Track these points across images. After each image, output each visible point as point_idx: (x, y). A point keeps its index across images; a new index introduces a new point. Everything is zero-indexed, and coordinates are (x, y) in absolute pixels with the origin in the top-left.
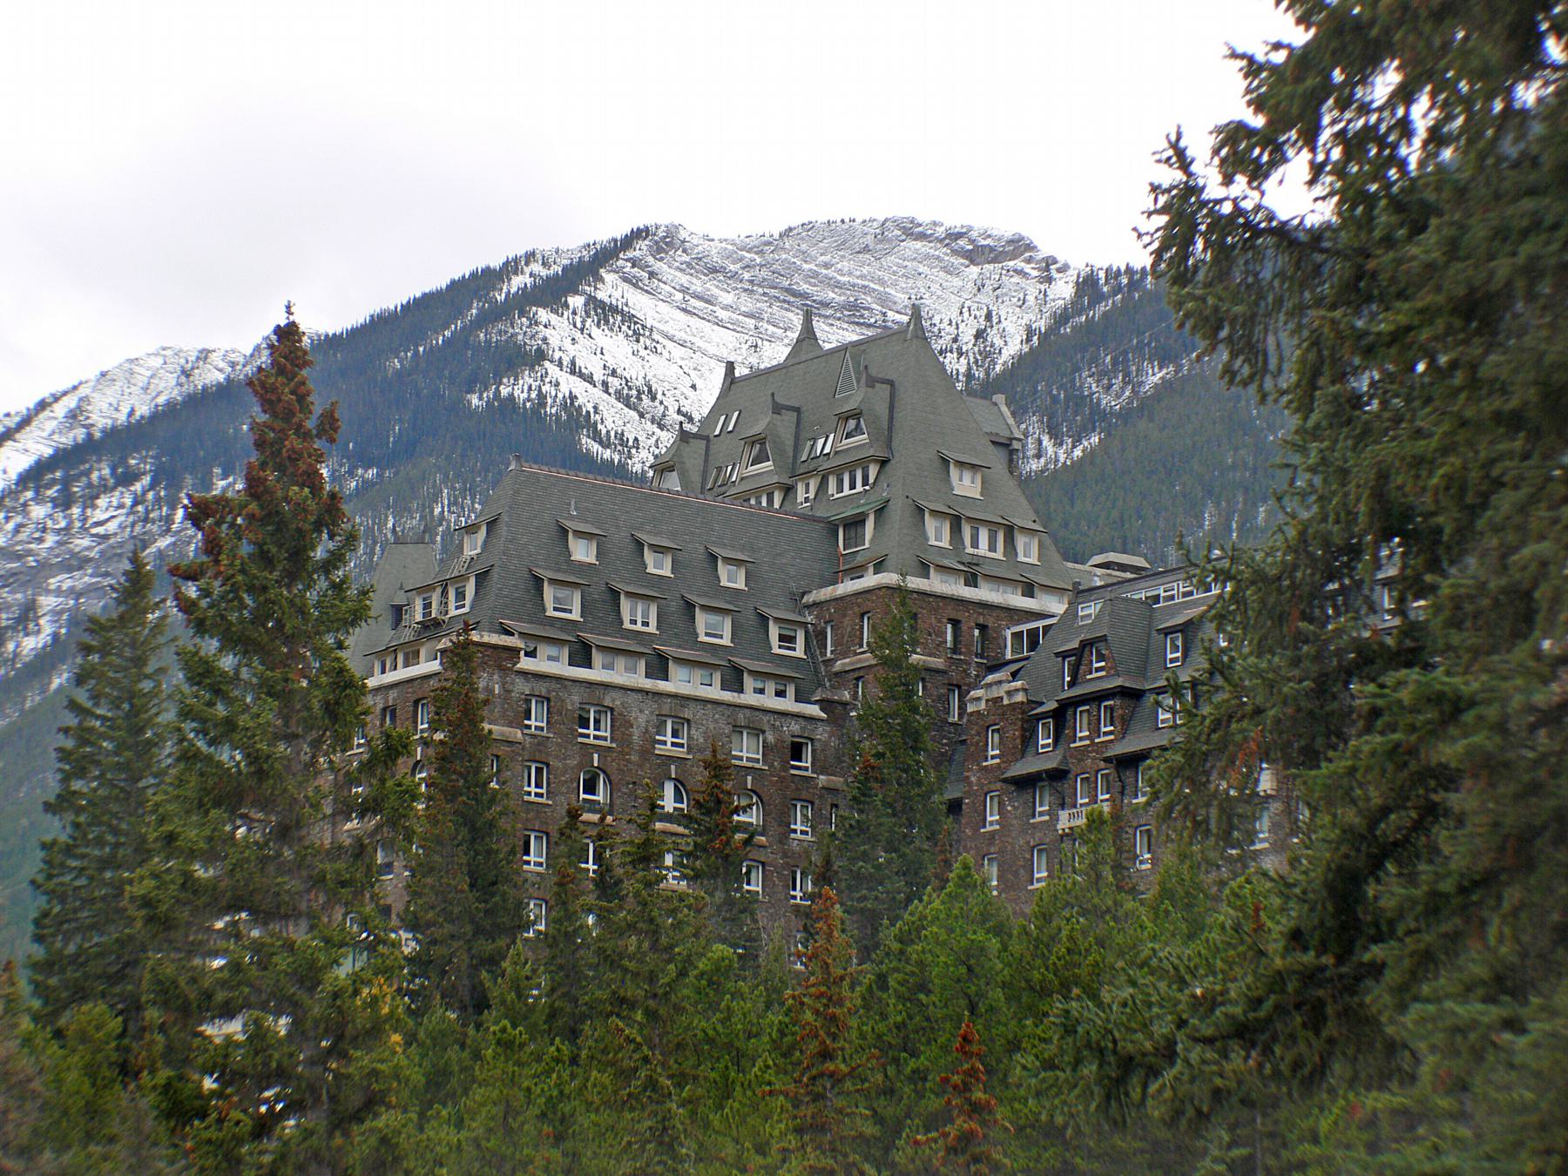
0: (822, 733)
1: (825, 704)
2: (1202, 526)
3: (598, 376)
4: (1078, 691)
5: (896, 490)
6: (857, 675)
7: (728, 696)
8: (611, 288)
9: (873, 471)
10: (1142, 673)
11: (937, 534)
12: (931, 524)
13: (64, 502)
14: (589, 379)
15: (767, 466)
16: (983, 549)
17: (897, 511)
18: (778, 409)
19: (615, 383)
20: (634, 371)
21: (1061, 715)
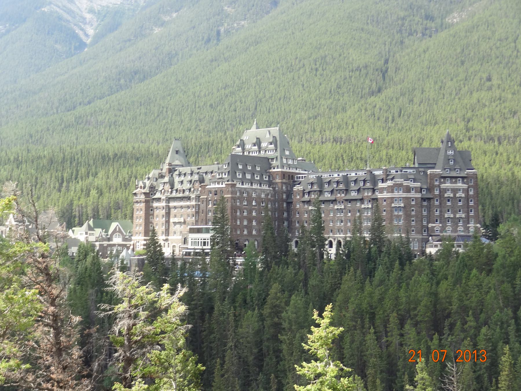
1: (272, 188)
4: (312, 190)
11: (285, 161)
14: (59, 7)
18: (257, 138)
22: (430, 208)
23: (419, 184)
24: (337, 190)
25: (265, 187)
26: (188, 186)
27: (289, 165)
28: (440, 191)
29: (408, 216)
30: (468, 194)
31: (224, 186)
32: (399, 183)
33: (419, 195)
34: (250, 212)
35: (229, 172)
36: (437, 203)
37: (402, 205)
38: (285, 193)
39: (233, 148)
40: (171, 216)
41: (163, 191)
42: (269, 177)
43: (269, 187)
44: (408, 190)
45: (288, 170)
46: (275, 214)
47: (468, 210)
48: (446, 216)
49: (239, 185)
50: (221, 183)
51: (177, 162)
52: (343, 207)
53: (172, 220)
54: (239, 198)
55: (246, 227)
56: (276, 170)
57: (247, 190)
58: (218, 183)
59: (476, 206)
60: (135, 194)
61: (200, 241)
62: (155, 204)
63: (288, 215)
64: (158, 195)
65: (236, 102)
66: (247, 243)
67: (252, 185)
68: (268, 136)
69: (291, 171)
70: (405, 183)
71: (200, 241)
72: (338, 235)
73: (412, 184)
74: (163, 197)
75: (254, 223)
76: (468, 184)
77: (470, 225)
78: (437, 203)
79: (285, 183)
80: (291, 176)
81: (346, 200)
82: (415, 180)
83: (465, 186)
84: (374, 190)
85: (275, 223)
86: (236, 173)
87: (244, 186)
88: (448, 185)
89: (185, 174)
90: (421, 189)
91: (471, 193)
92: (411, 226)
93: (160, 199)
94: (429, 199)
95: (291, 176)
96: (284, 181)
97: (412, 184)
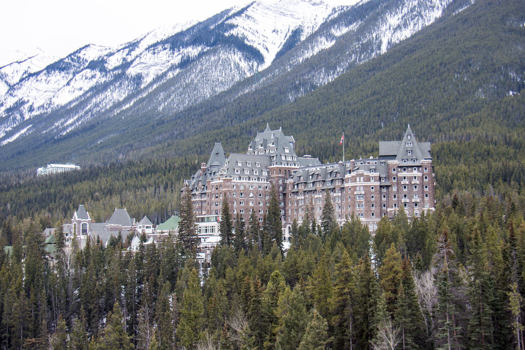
0: (269, 185)
1: (270, 181)
3: (248, 29)
6: (274, 178)
7: (258, 182)
8: (249, 12)
10: (307, 180)
11: (283, 158)
13: (154, 53)
15: (263, 147)
16: (289, 160)
17: (278, 156)
19: (251, 31)
20: (254, 27)
21: (297, 184)
24: (317, 182)
27: (288, 161)
28: (397, 178)
29: (367, 201)
30: (423, 181)
31: (222, 181)
33: (378, 184)
34: (247, 203)
35: (228, 169)
37: (363, 193)
40: (203, 209)
42: (268, 172)
43: (267, 181)
44: (368, 179)
45: (286, 166)
47: (423, 196)
49: (236, 180)
52: (321, 196)
54: (235, 191)
56: (275, 166)
57: (244, 184)
60: (182, 191)
63: (285, 204)
65: (380, 107)
68: (272, 137)
69: (289, 166)
70: (366, 173)
74: (197, 193)
79: (282, 177)
81: (323, 190)
82: (375, 170)
84: (343, 180)
88: (404, 174)
89: (214, 173)
90: (380, 178)
91: (425, 180)
93: (195, 194)
94: (388, 187)
96: (280, 175)
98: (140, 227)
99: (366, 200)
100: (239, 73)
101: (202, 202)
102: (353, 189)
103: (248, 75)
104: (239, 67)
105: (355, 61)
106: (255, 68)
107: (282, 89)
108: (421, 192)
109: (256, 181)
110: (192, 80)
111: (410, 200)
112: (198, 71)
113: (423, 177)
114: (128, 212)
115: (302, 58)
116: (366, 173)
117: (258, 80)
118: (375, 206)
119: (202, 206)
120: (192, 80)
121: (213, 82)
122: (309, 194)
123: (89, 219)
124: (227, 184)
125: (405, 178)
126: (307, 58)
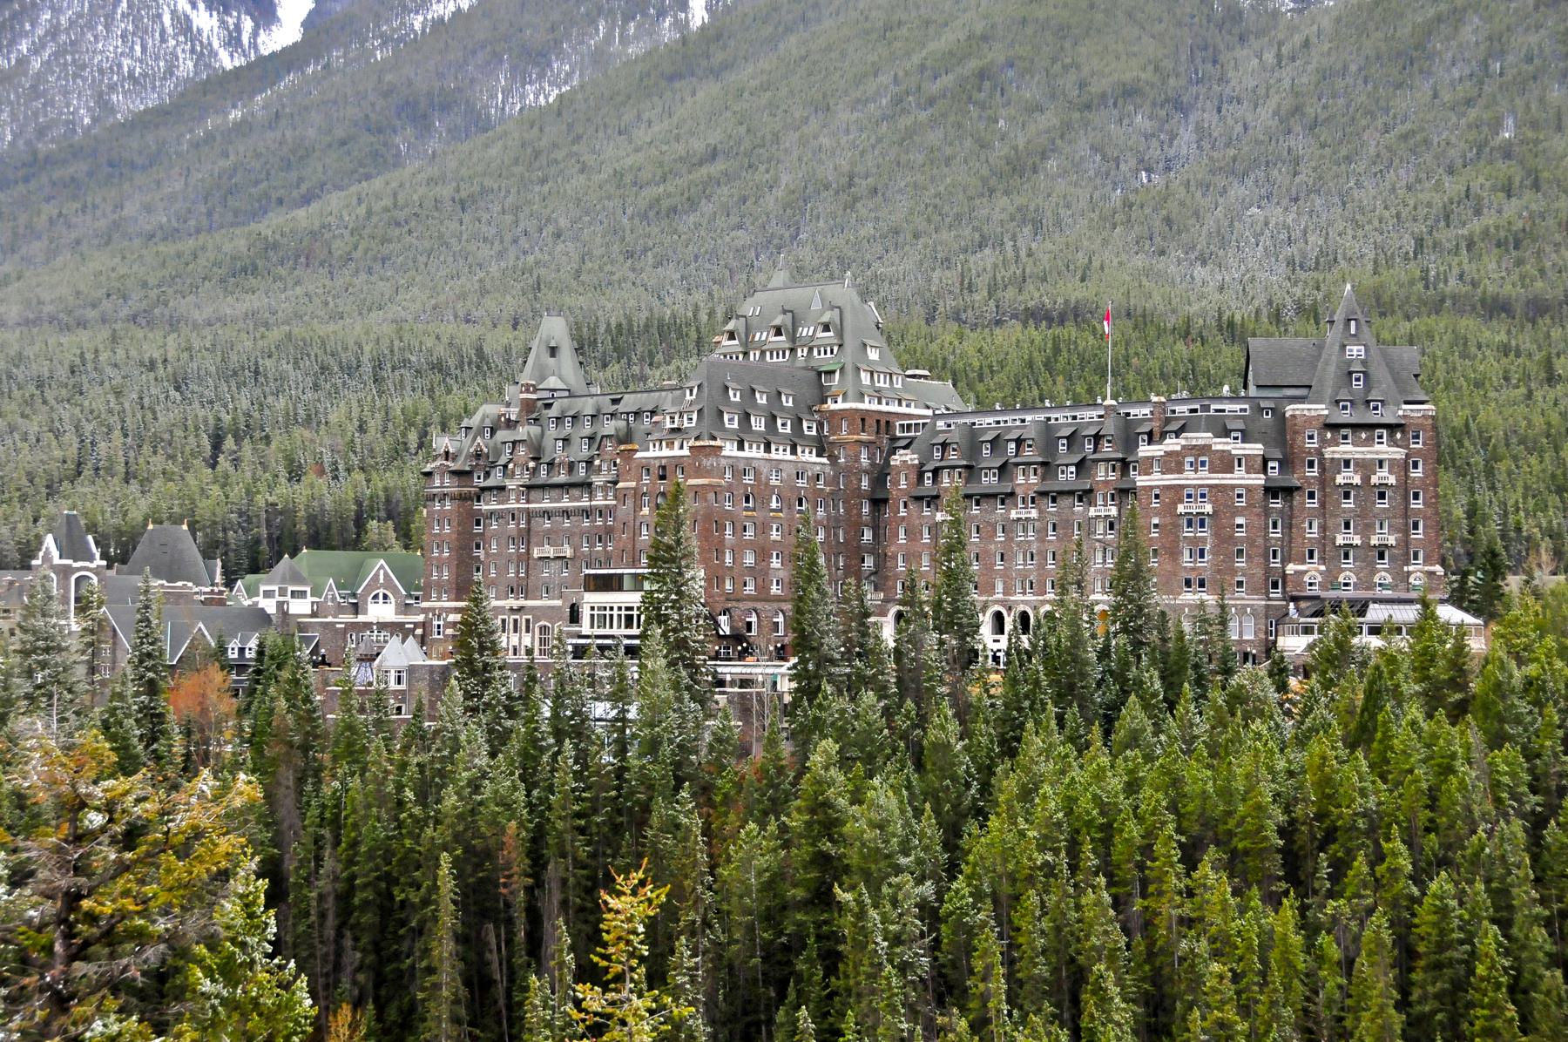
0: (827, 470)
1: (829, 457)
2: (597, 30)
5: (848, 358)
6: (842, 444)
9: (836, 349)
11: (865, 378)
12: (863, 374)
17: (849, 368)
21: (936, 472)
22: (1291, 517)
23: (1260, 446)
24: (1017, 465)
25: (808, 456)
26: (585, 451)
27: (878, 391)
28: (1322, 465)
29: (1224, 539)
30: (1407, 476)
31: (686, 452)
32: (1200, 442)
33: (1258, 480)
34: (763, 529)
35: (700, 411)
36: (1314, 504)
37: (1208, 508)
38: (866, 472)
39: (717, 339)
40: (534, 540)
41: (511, 466)
42: (820, 425)
43: (819, 455)
44: (1226, 463)
45: (875, 407)
46: (837, 535)
47: (1407, 524)
48: (1340, 540)
49: (730, 449)
50: (677, 444)
51: (553, 382)
52: (1034, 514)
53: (536, 553)
54: (730, 488)
55: (751, 570)
56: (840, 405)
58: (670, 445)
59: (1430, 512)
61: (615, 613)
62: (488, 505)
64: (496, 478)
66: (754, 619)
67: (768, 449)
69: (883, 408)
70: (1220, 444)
71: (615, 613)
72: (1019, 597)
73: (1237, 448)
75: (775, 563)
76: (1407, 447)
77: (1411, 568)
78: (1314, 504)
79: (867, 444)
80: (883, 423)
82: (1246, 437)
83: (1398, 453)
84: (1124, 465)
85: (837, 562)
86: (721, 413)
87: (746, 454)
88: (1346, 450)
89: (573, 417)
90: (1265, 461)
92: (1234, 572)
93: (502, 488)
94: (1289, 492)
95: (883, 423)
96: (864, 437)
97: (1237, 448)
98: (268, 594)
99: (1216, 535)
100: (193, 51)
101: (530, 515)
102: (1171, 494)
103: (227, 61)
104: (189, 28)
105: (609, 38)
106: (245, 38)
107: (372, 116)
108: (1399, 511)
109: (789, 457)
110: (23, 62)
111: (1365, 538)
112: (40, 32)
113: (1406, 461)
114: (318, 547)
115: (420, 18)
116: (1220, 444)
117: (278, 78)
118: (1249, 556)
119: (529, 530)
120: (23, 62)
121: (101, 71)
122: (984, 505)
123: (99, 562)
124: (708, 462)
125: (1347, 463)
126: (441, 19)
